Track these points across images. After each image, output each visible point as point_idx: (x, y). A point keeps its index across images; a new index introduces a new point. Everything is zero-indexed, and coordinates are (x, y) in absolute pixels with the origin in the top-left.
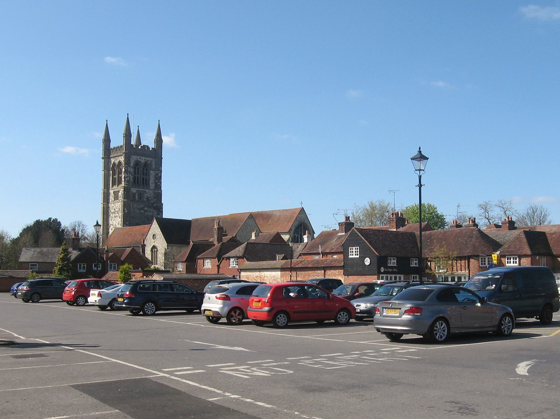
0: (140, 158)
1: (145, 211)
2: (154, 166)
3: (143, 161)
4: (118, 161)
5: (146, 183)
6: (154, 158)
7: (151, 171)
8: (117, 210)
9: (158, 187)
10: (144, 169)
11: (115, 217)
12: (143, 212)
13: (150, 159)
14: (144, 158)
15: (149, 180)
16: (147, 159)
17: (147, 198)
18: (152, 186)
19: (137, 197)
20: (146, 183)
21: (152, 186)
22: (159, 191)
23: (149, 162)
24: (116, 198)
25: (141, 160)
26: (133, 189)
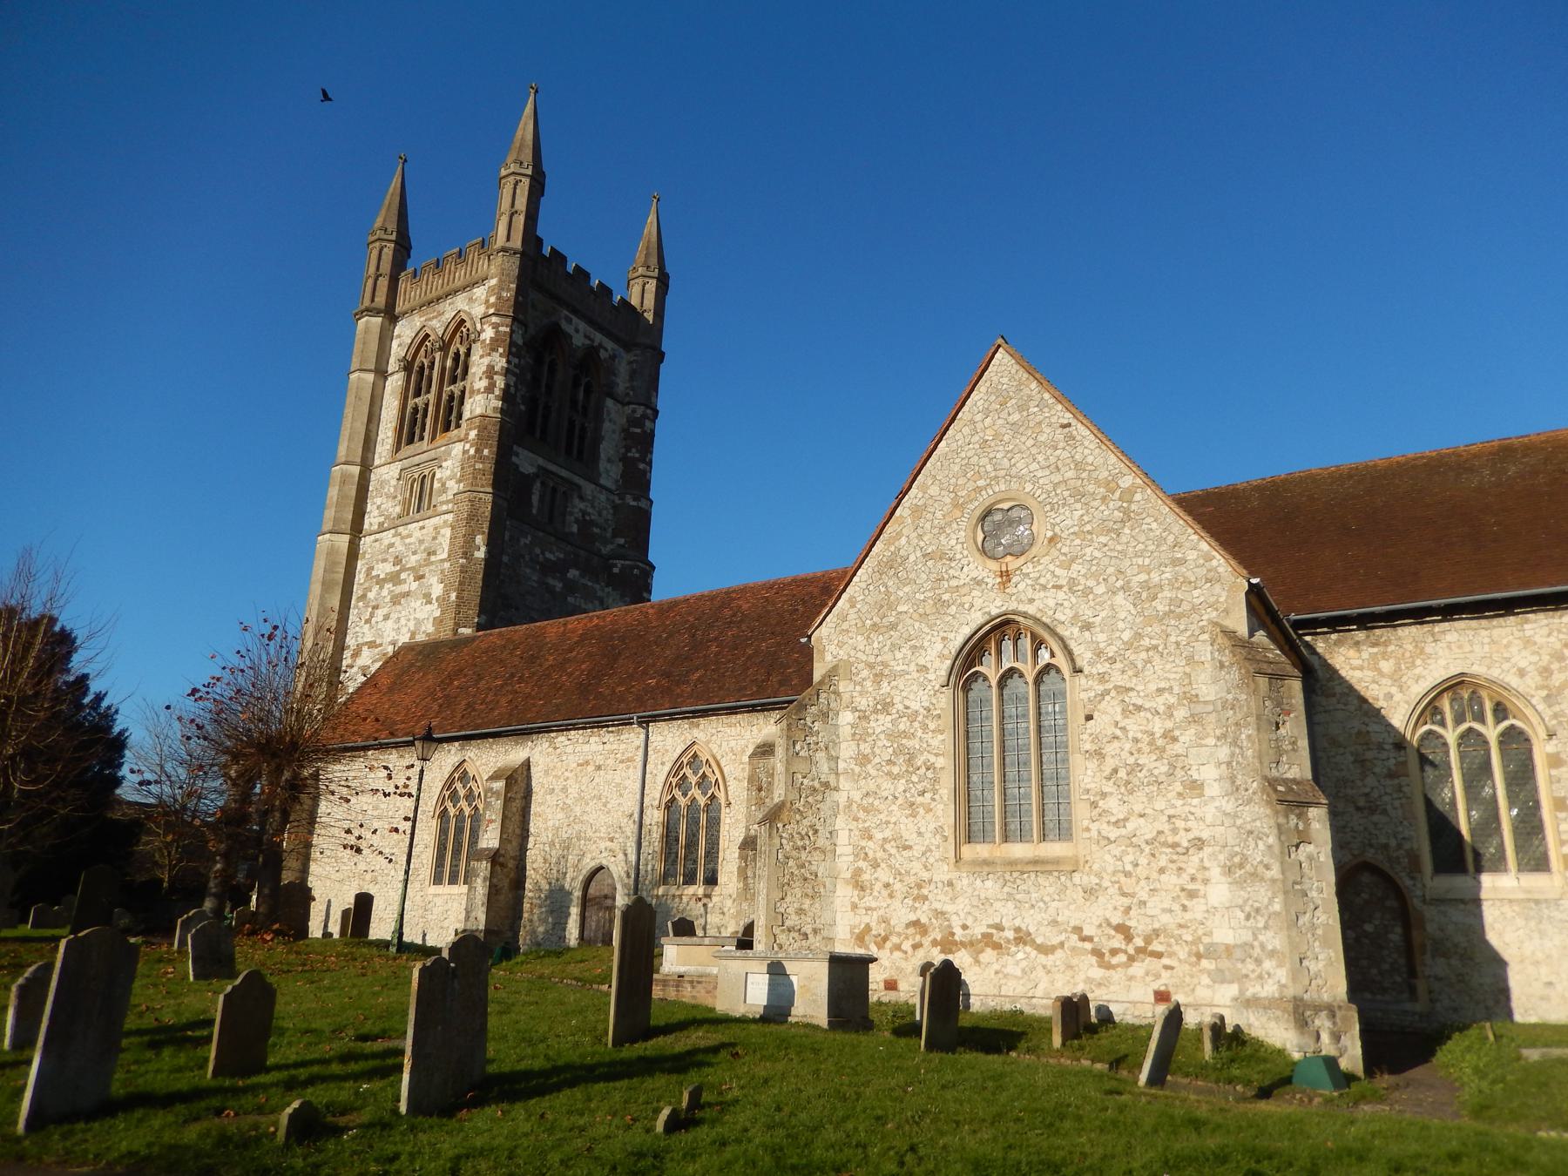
0: (569, 321)
1: (571, 587)
2: (622, 384)
3: (578, 341)
4: (449, 315)
5: (580, 452)
6: (627, 347)
7: (609, 402)
8: (413, 560)
9: (637, 480)
10: (576, 384)
11: (396, 600)
12: (559, 586)
13: (610, 345)
14: (582, 326)
15: (597, 440)
16: (599, 338)
17: (585, 524)
18: (610, 472)
19: (535, 499)
20: (580, 452)
21: (610, 472)
22: (643, 504)
23: (603, 354)
24: (420, 495)
25: (569, 329)
26: (523, 453)
